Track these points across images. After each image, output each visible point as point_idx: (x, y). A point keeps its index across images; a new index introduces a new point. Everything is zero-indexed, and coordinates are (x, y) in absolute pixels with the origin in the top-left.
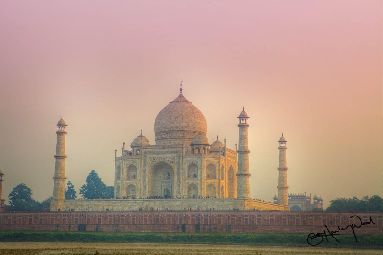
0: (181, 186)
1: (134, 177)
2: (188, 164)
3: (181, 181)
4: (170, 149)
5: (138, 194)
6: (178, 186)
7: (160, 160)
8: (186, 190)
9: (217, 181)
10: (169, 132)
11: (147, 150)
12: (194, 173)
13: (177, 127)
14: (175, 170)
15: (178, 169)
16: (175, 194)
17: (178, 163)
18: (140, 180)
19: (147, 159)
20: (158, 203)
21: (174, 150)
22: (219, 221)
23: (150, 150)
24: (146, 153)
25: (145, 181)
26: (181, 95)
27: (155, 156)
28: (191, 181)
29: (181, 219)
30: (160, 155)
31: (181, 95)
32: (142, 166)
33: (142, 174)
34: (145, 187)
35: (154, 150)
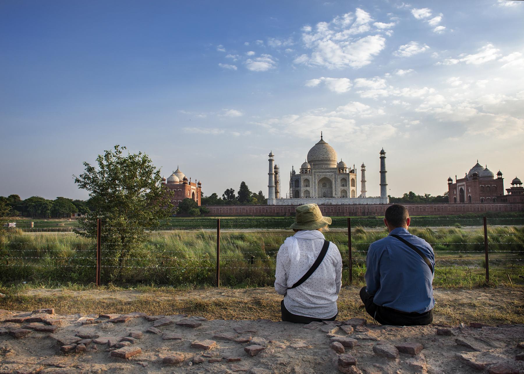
1: (307, 186)
5: (311, 195)
6: (336, 191)
8: (340, 193)
10: (322, 160)
14: (334, 182)
15: (335, 182)
16: (334, 195)
17: (335, 178)
20: (334, 200)
21: (332, 170)
22: (376, 210)
23: (318, 171)
24: (315, 172)
25: (315, 188)
26: (322, 140)
28: (343, 188)
29: (354, 209)
31: (322, 140)
35: (320, 171)
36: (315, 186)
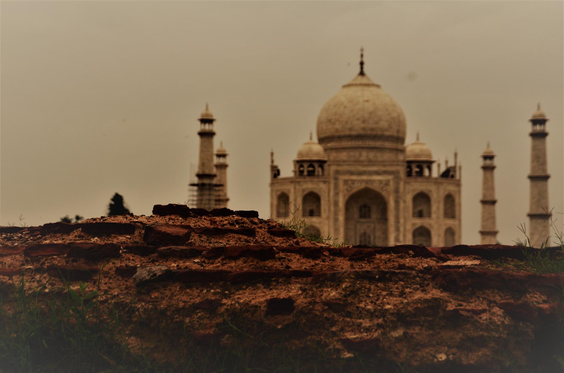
0: (402, 229)
1: (312, 214)
2: (415, 193)
3: (402, 221)
4: (382, 169)
7: (363, 186)
9: (457, 222)
10: (359, 137)
11: (340, 168)
12: (419, 208)
13: (372, 129)
14: (391, 204)
15: (397, 202)
17: (397, 191)
18: (328, 218)
19: (341, 183)
25: (336, 220)
27: (354, 177)
28: (419, 222)
30: (365, 177)
32: (332, 193)
33: (332, 208)
34: (336, 230)
35: (352, 168)
36: (336, 213)
